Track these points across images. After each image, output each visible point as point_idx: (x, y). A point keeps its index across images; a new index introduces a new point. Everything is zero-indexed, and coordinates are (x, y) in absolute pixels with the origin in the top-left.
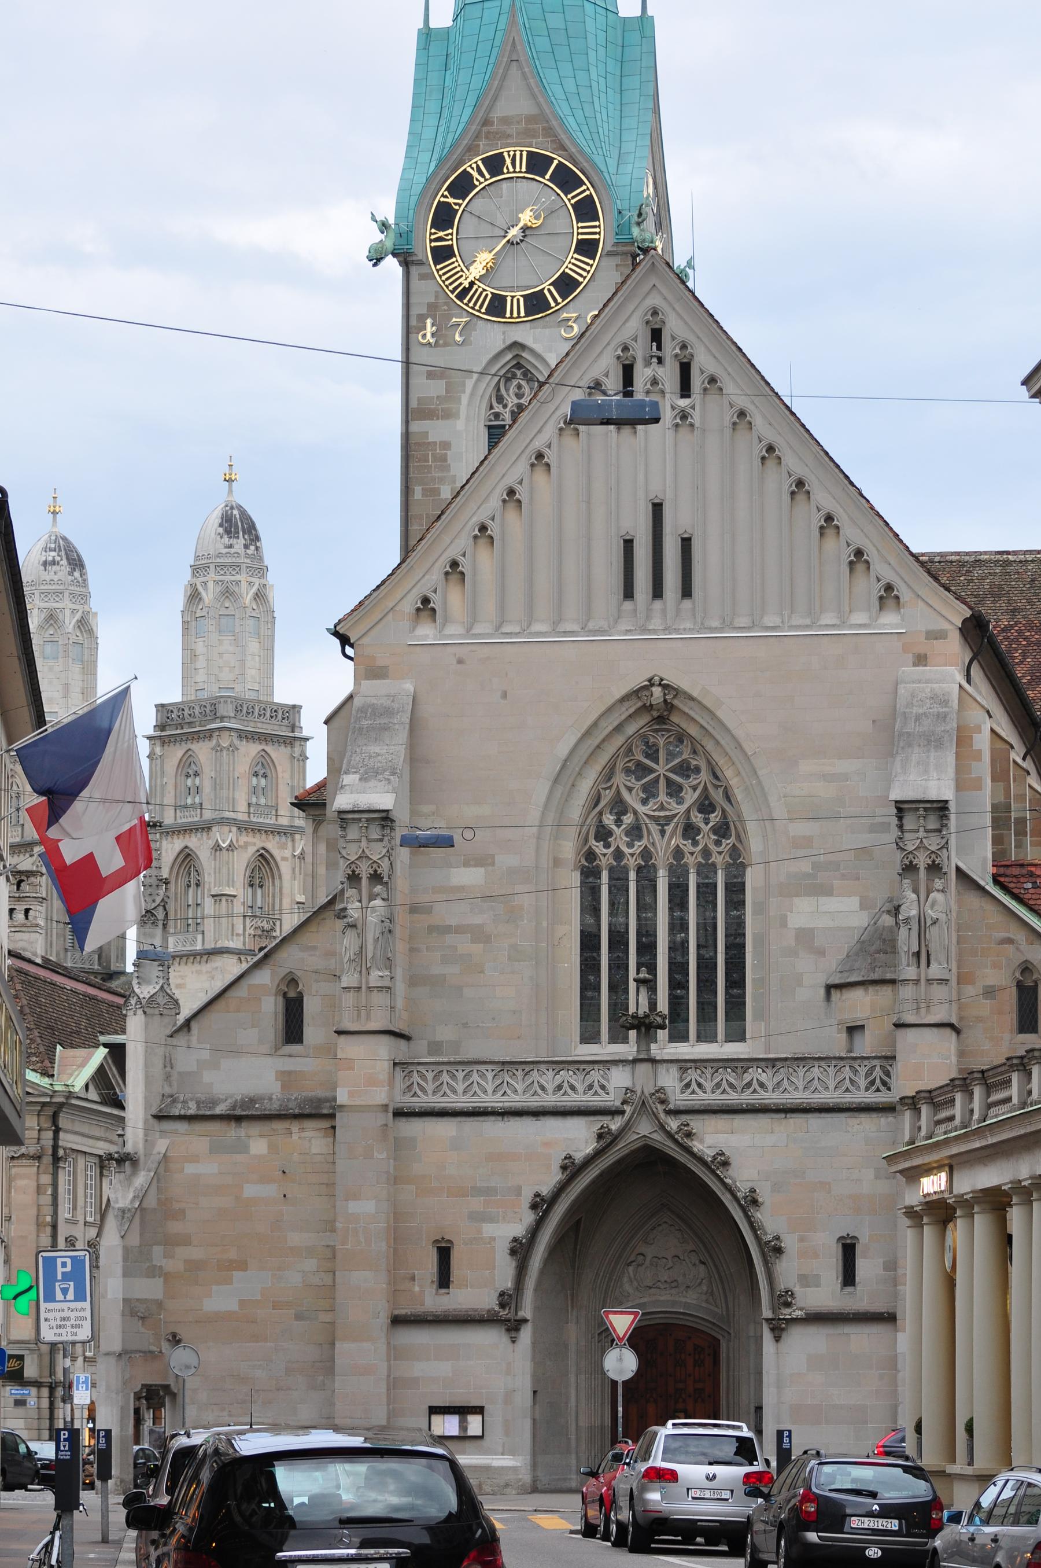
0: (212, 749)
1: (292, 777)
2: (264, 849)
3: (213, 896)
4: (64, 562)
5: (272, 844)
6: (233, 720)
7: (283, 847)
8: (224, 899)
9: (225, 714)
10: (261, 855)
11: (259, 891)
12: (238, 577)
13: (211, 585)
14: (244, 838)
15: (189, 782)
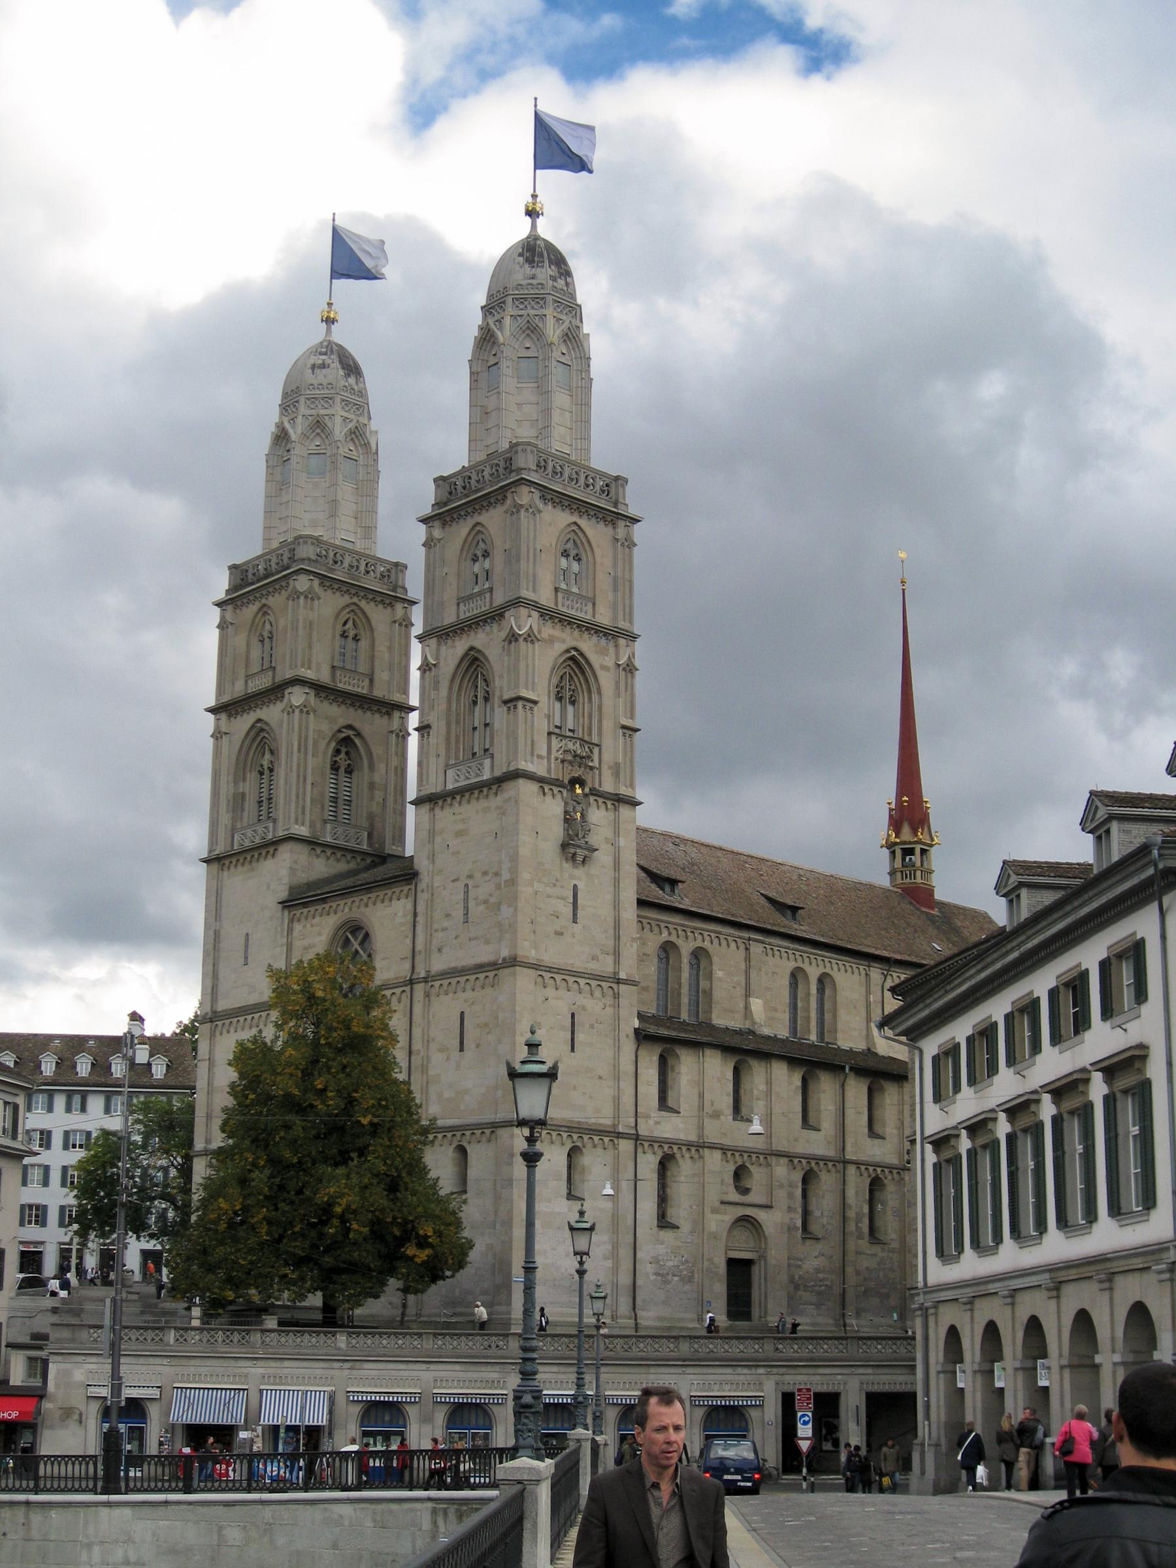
0: (506, 512)
1: (615, 565)
2: (576, 649)
3: (506, 702)
4: (337, 364)
5: (588, 645)
6: (533, 474)
7: (603, 652)
8: (520, 704)
9: (522, 465)
10: (572, 658)
11: (570, 709)
12: (543, 311)
13: (507, 321)
14: (549, 630)
15: (477, 568)
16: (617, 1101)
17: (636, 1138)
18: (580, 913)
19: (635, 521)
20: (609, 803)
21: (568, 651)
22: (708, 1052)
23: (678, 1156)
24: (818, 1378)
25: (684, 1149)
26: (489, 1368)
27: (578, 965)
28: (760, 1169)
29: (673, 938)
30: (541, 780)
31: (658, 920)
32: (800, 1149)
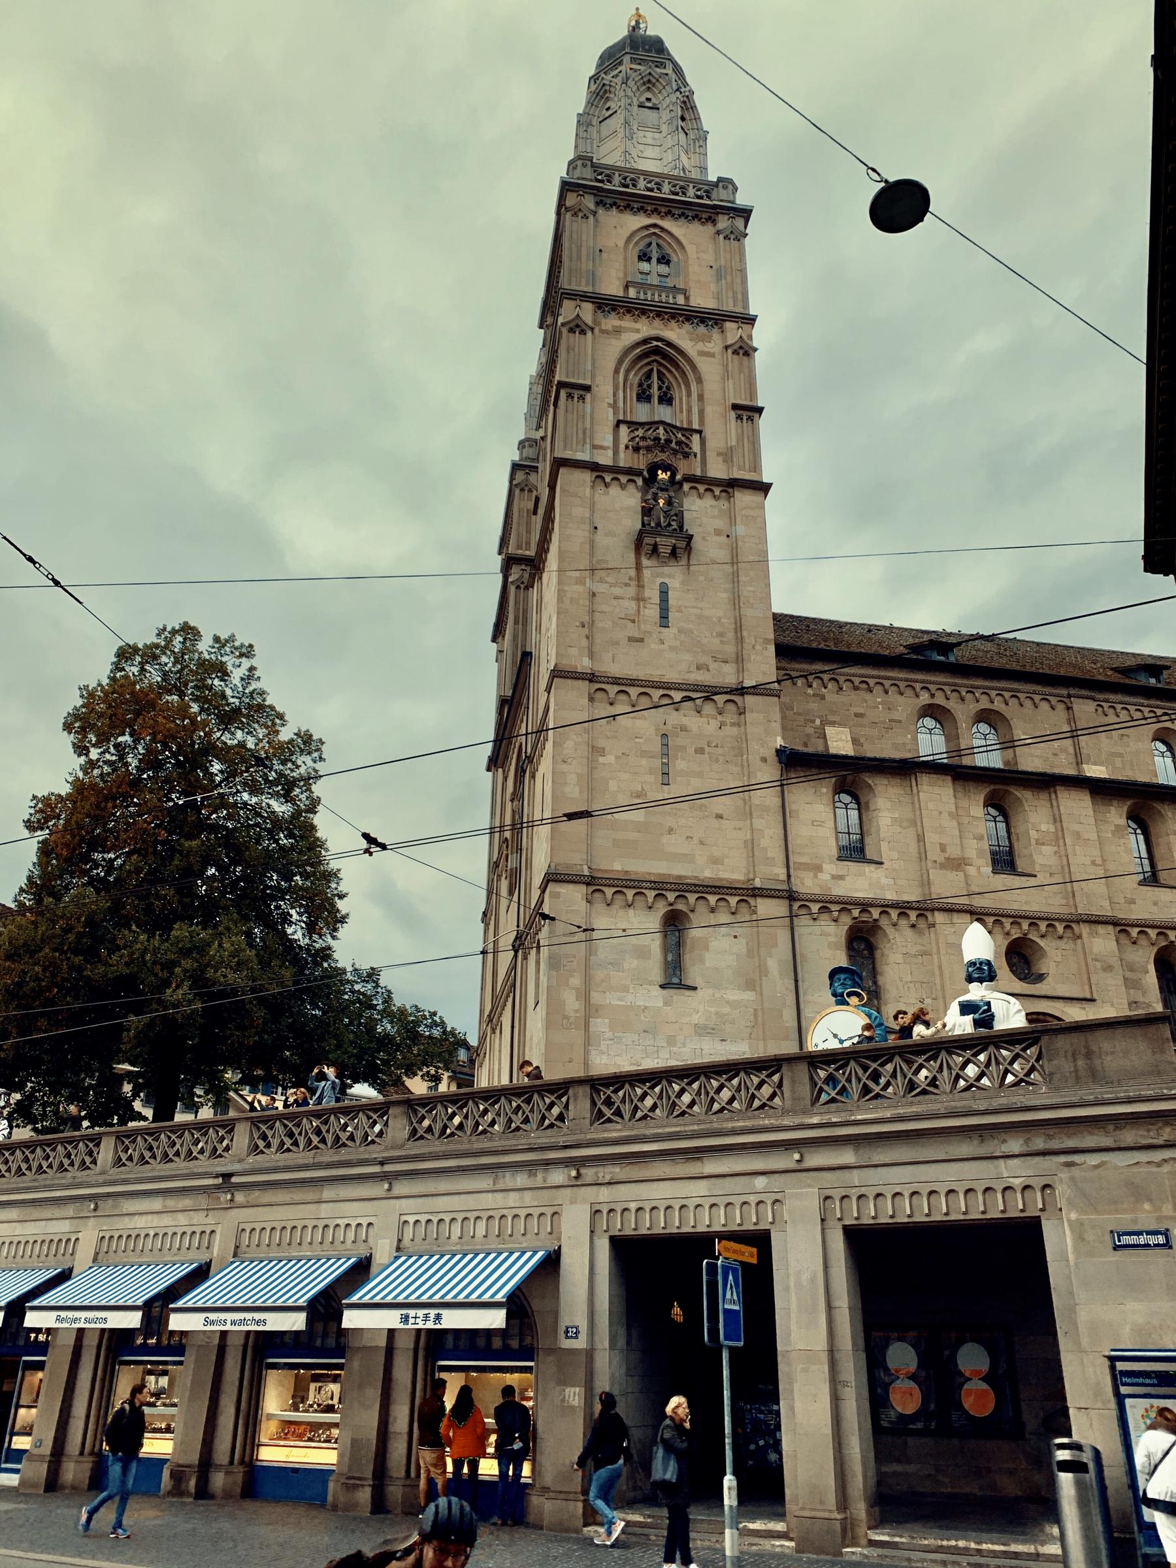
2: (658, 339)
10: (657, 351)
16: (751, 846)
17: (791, 896)
18: (672, 615)
19: (745, 213)
20: (717, 491)
21: (645, 341)
22: (925, 779)
23: (884, 923)
24: (701, 1188)
25: (894, 914)
26: (57, 1212)
27: (671, 676)
28: (1061, 944)
29: (940, 700)
30: (594, 467)
31: (906, 680)
32: (1138, 913)
